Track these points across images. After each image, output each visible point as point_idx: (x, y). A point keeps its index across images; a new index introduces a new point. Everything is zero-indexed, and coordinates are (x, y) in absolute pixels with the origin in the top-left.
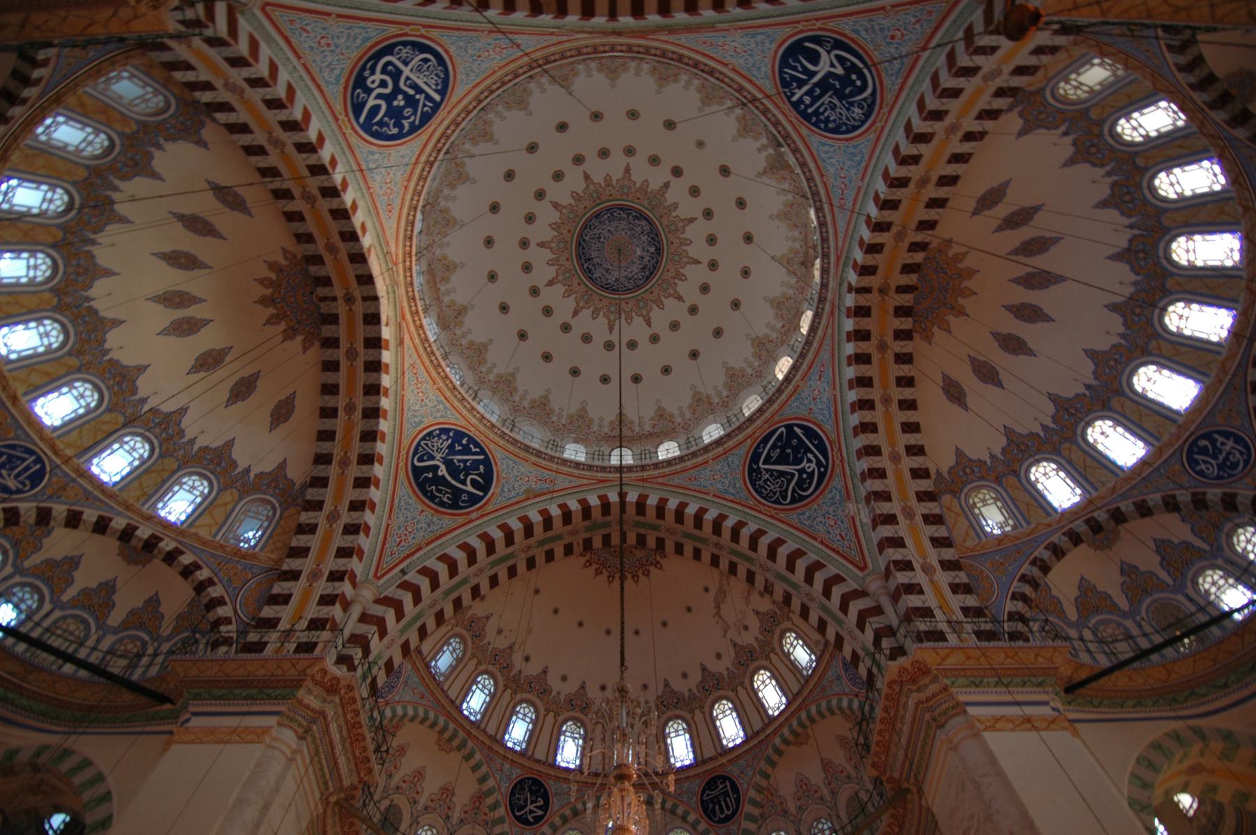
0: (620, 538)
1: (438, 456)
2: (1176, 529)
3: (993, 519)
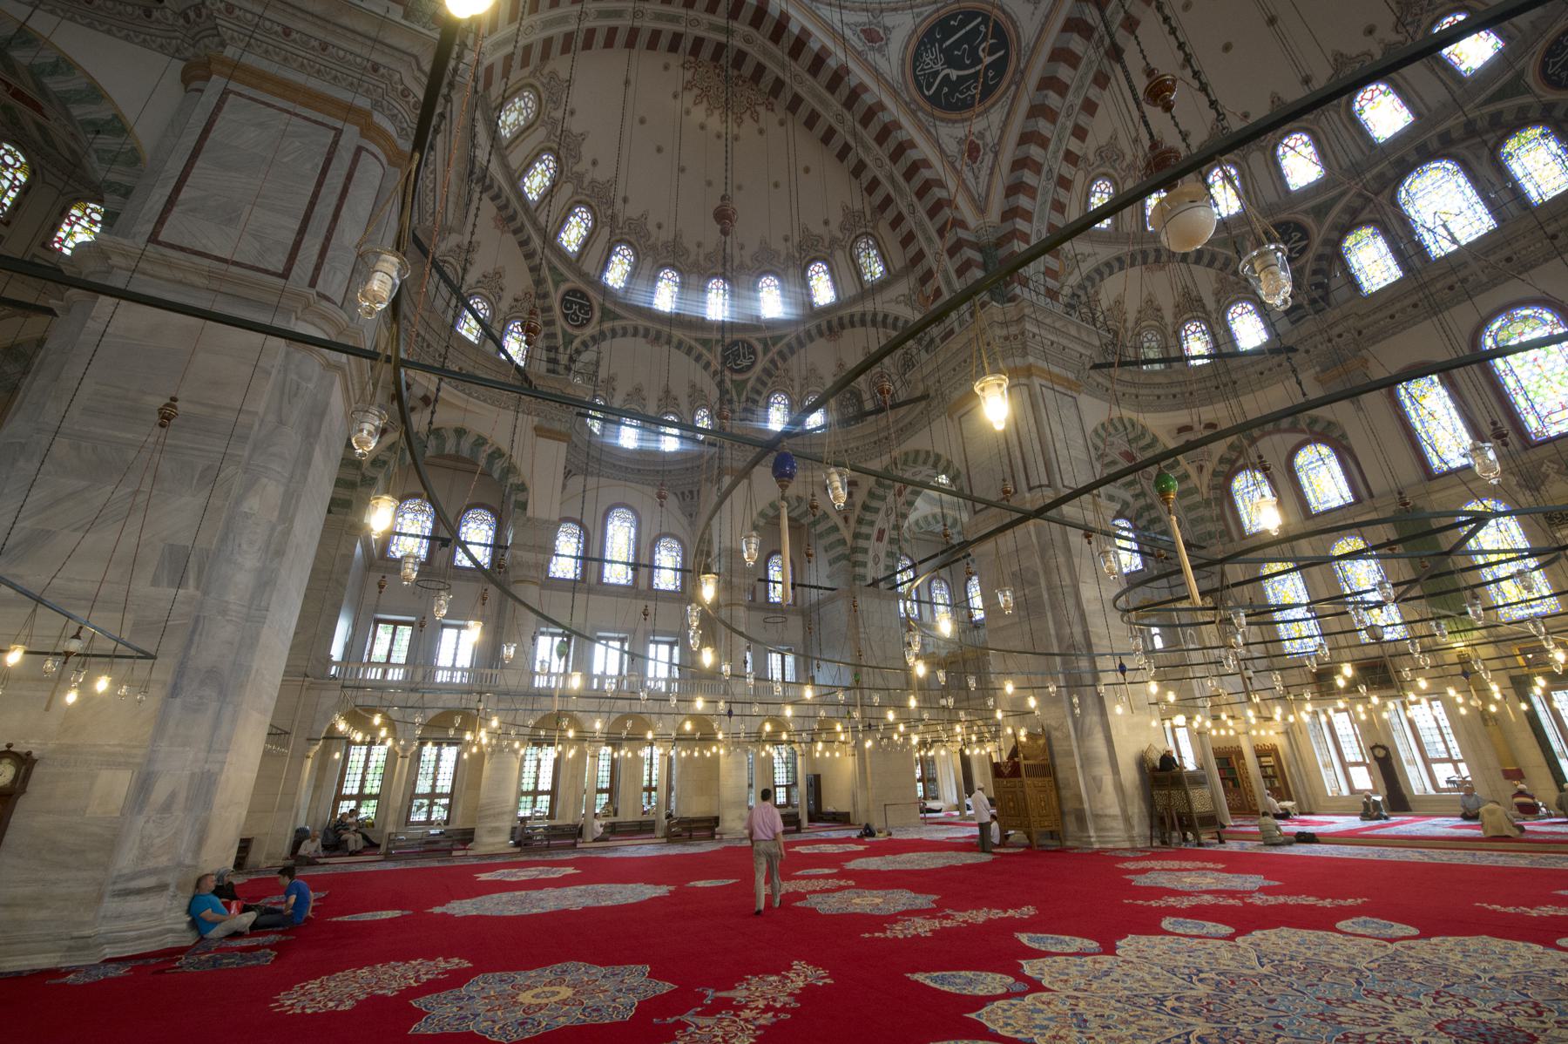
1: (938, 67)
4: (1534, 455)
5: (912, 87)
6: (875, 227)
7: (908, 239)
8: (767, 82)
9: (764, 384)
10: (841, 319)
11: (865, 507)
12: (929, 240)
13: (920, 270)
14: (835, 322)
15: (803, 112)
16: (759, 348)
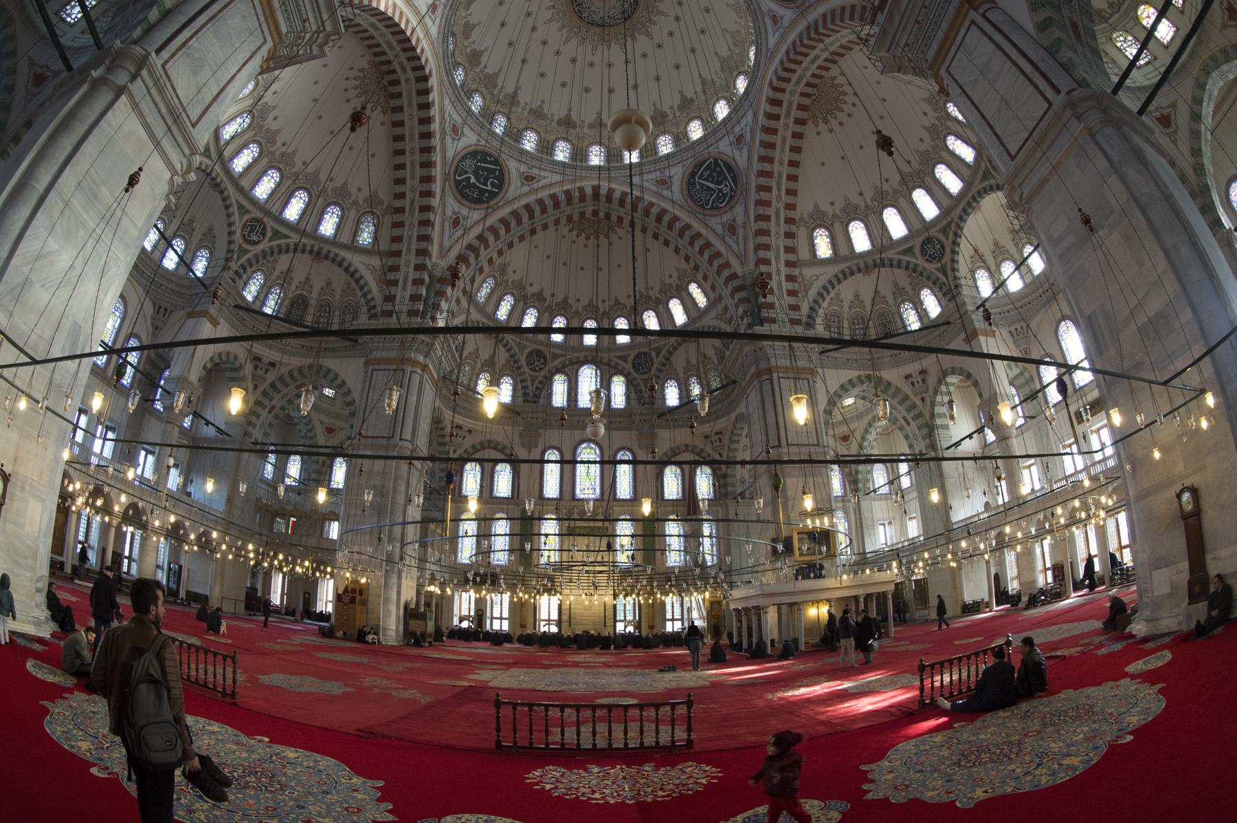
0: (596, 214)
2: (902, 276)
3: (823, 248)
4: (575, 503)
5: (453, 168)
6: (383, 216)
7: (397, 239)
8: (395, 103)
9: (258, 261)
10: (329, 252)
11: (273, 385)
12: (409, 250)
13: (392, 261)
14: (324, 252)
15: (398, 131)
16: (269, 234)
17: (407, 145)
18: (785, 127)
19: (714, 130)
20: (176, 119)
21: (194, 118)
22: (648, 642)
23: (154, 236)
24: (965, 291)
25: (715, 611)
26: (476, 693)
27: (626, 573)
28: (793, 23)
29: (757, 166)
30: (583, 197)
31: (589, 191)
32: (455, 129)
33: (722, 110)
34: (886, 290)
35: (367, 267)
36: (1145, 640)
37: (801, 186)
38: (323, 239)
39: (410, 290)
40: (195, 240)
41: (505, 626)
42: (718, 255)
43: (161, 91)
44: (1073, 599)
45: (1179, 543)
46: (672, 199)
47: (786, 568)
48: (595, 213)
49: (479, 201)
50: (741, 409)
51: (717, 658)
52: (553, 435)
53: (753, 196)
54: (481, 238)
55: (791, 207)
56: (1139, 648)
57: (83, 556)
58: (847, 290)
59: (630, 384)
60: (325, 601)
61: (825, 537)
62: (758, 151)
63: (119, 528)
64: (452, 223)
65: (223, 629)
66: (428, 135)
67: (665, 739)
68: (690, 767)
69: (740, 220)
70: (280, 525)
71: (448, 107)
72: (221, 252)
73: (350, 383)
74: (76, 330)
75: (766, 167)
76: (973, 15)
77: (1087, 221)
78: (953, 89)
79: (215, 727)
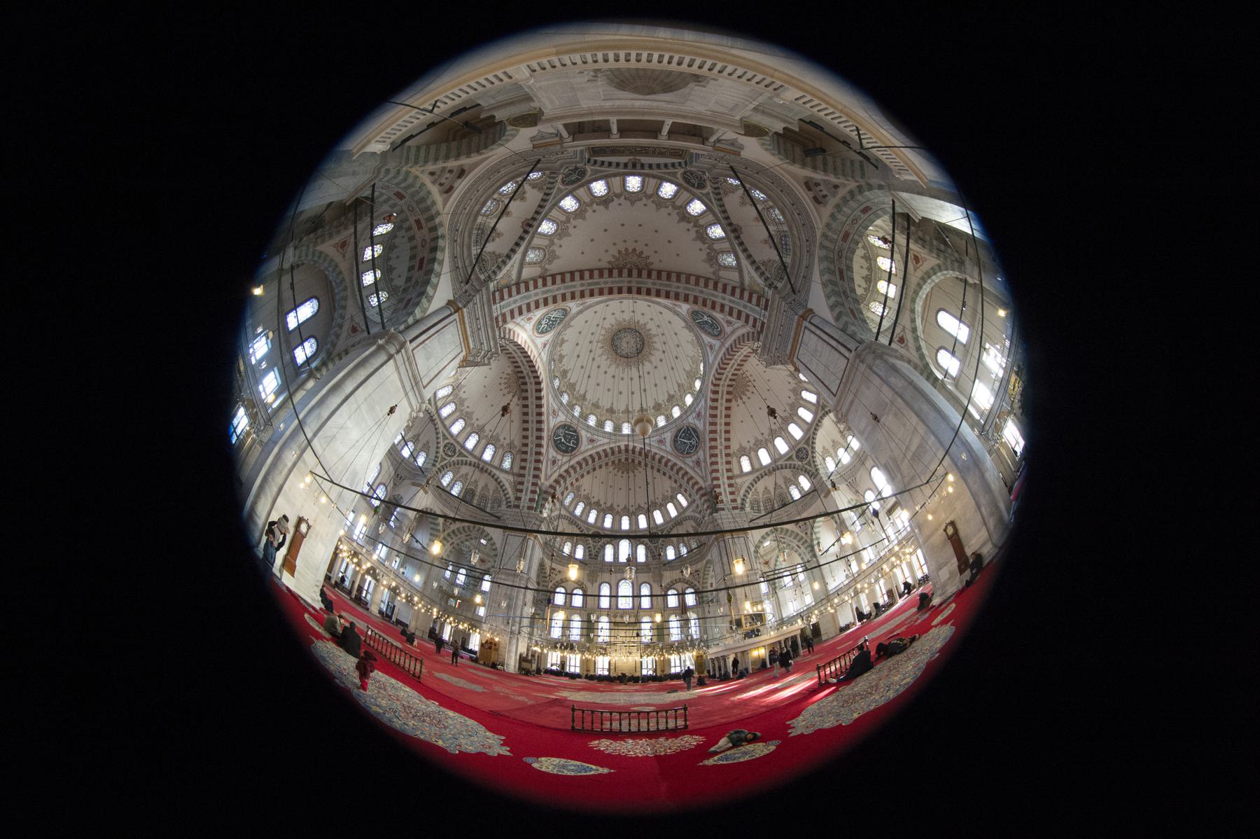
0: (627, 461)
2: (787, 473)
8: (524, 394)
13: (520, 479)
17: (530, 418)
18: (722, 404)
19: (686, 411)
20: (417, 384)
21: (425, 381)
22: (661, 678)
23: (400, 437)
24: (821, 471)
25: (700, 662)
26: (561, 702)
27: (647, 646)
28: (720, 348)
29: (708, 428)
30: (620, 451)
31: (623, 448)
32: (554, 411)
33: (689, 400)
34: (781, 482)
35: (507, 480)
36: (941, 605)
37: (732, 436)
38: (485, 462)
39: (529, 495)
40: (420, 446)
41: (578, 670)
42: (692, 478)
43: (410, 364)
44: (900, 602)
45: (950, 550)
46: (666, 450)
47: (739, 636)
48: (627, 459)
49: (566, 451)
50: (709, 557)
51: (701, 683)
52: (606, 576)
53: (708, 445)
54: (567, 471)
55: (728, 447)
56: (937, 610)
57: (343, 579)
58: (760, 486)
59: (647, 548)
60: (475, 643)
61: (759, 617)
62: (709, 419)
63: (363, 575)
64: (552, 464)
65: (415, 643)
66: (540, 414)
67: (671, 725)
68: (687, 738)
69: (702, 458)
70: (452, 602)
71: (551, 400)
72: (432, 456)
73: (495, 539)
74: (355, 474)
75: (713, 428)
76: (805, 323)
77: (876, 418)
78: (801, 367)
79: (408, 689)
